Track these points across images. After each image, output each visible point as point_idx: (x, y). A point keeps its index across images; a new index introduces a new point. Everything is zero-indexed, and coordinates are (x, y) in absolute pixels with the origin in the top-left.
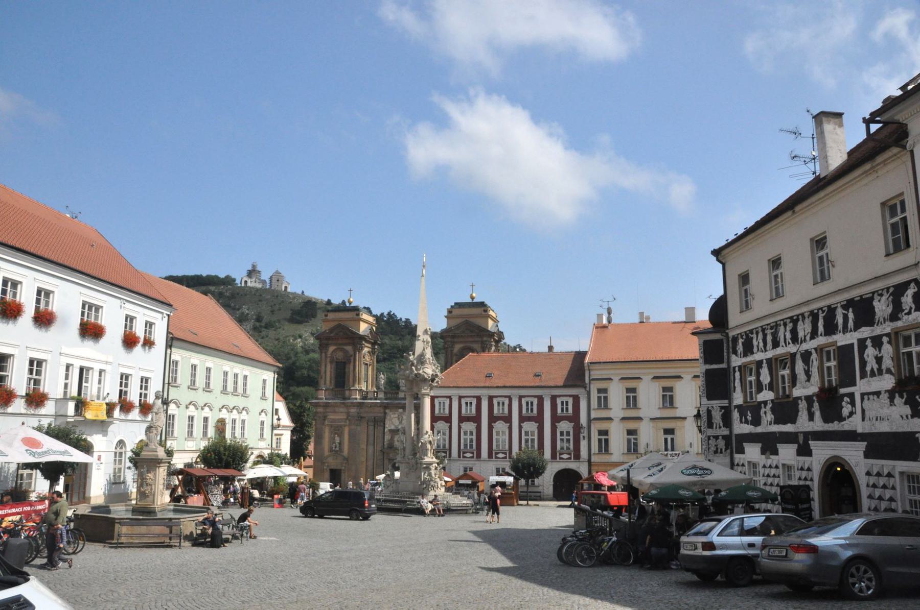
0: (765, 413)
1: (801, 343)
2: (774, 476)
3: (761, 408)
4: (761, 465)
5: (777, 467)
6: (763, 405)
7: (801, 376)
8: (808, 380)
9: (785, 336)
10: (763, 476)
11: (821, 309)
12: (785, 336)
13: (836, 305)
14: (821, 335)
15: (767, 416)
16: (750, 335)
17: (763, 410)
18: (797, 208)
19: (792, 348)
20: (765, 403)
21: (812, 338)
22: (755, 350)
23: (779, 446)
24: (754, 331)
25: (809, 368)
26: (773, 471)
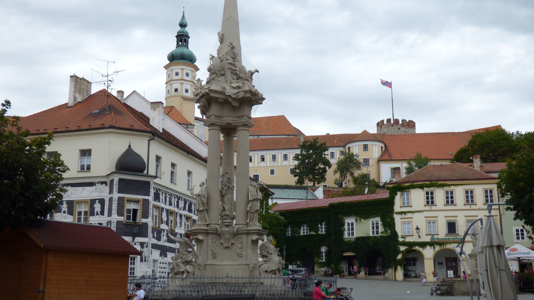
0: (163, 235)
1: (180, 210)
2: (164, 268)
3: (161, 232)
4: (159, 262)
5: (166, 263)
6: (162, 231)
7: (178, 224)
8: (181, 227)
9: (174, 203)
10: (159, 268)
11: (188, 200)
12: (174, 203)
13: (192, 203)
14: (187, 211)
15: (164, 238)
16: (158, 191)
17: (162, 234)
18: (189, 156)
19: (176, 210)
20: (164, 230)
21: (183, 210)
22: (161, 200)
23: (168, 253)
24: (161, 191)
25: (181, 221)
26: (164, 265)
